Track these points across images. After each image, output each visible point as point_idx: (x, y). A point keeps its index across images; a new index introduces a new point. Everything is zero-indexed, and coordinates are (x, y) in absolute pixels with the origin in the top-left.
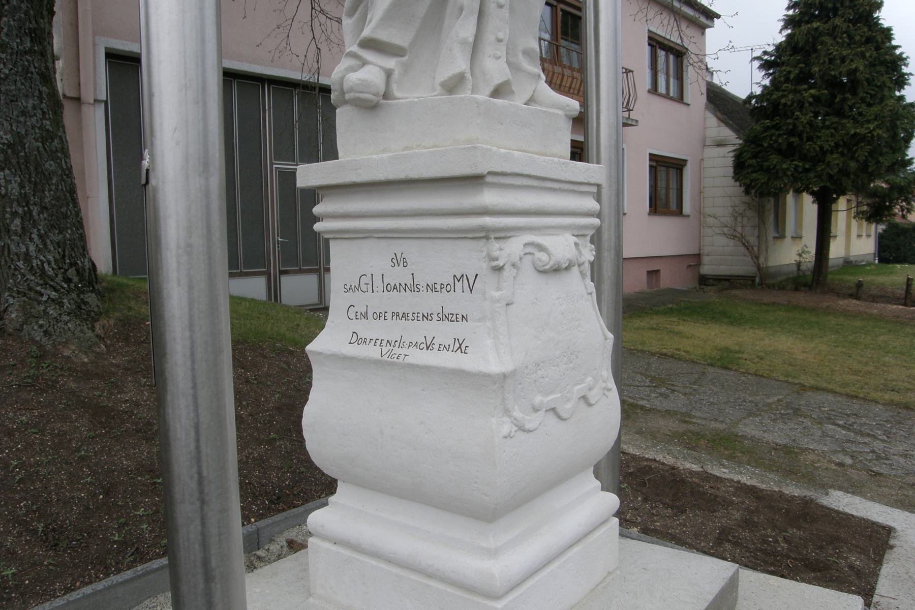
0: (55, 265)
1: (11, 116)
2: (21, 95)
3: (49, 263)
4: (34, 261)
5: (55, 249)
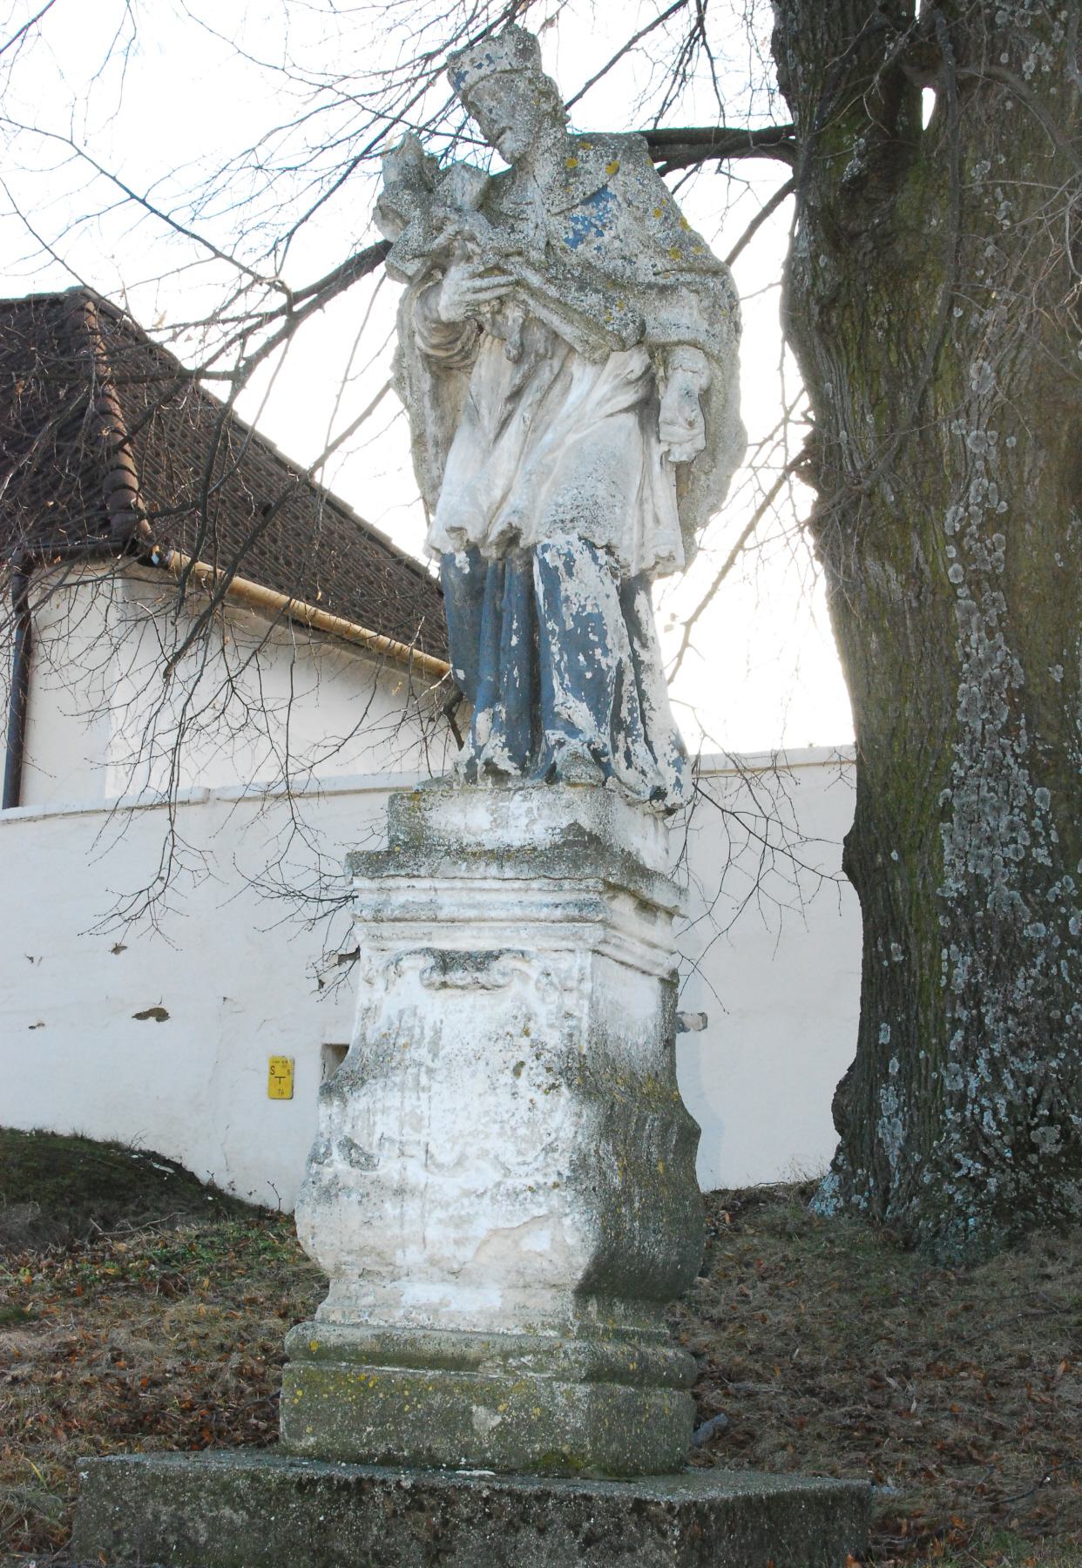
0: (1007, 1116)
2: (987, 809)
3: (995, 1113)
4: (969, 1106)
5: (1017, 1087)
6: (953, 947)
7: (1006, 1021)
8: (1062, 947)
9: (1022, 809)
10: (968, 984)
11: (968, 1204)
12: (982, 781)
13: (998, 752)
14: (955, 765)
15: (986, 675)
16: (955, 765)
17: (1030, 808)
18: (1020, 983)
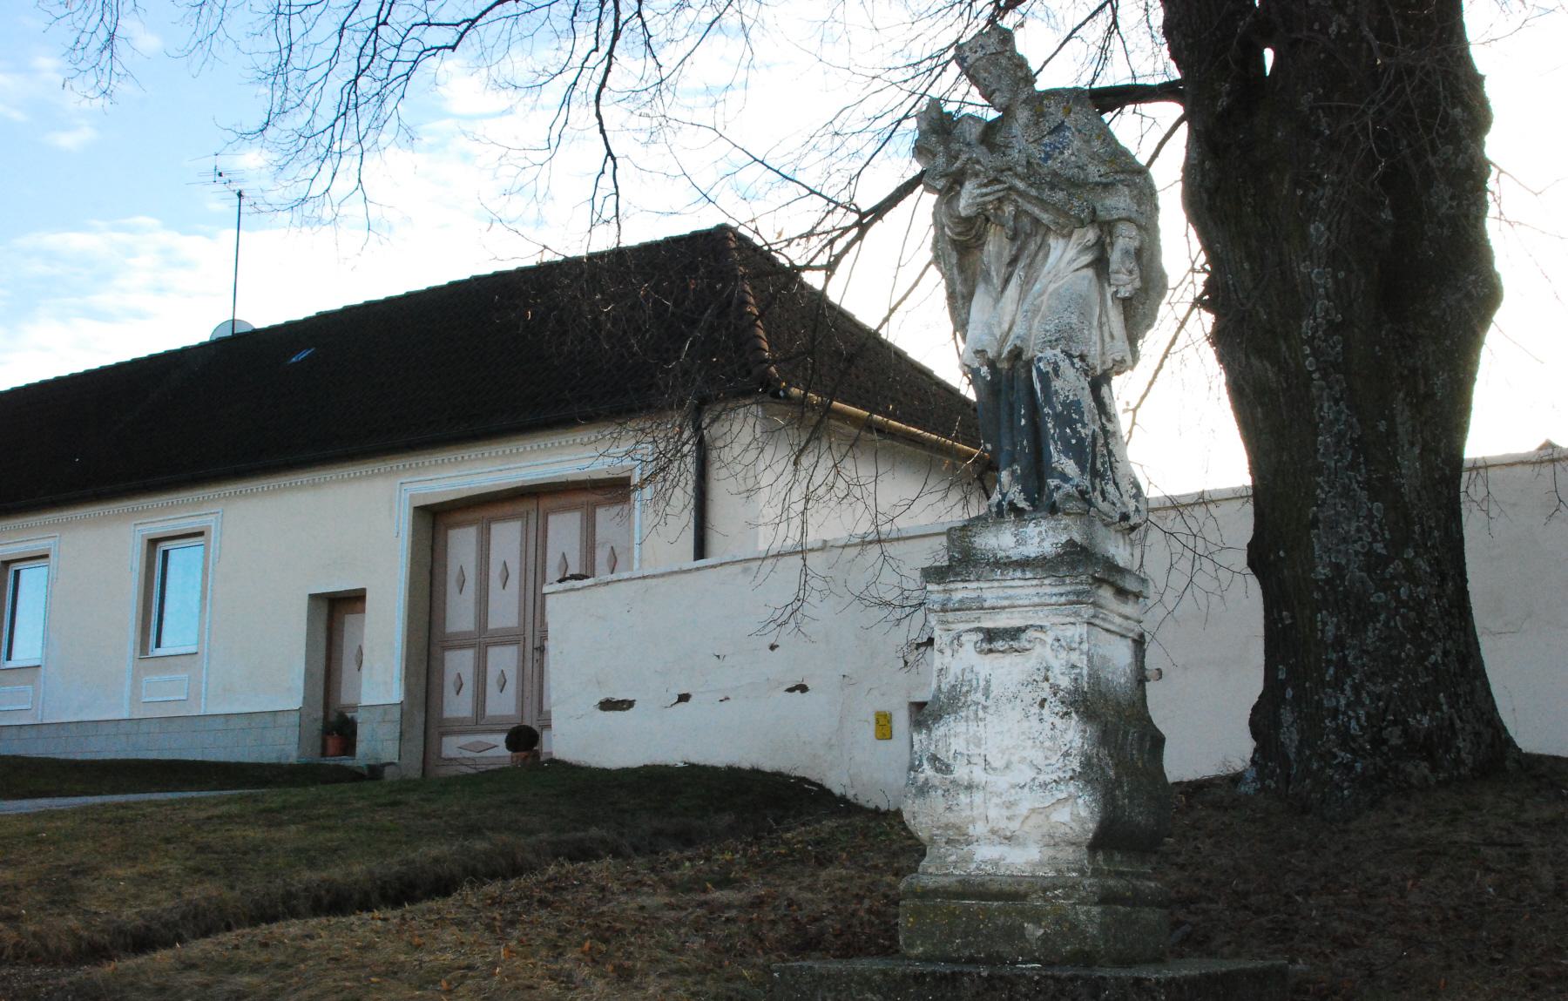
1: (1330, 546)
2: (1341, 519)
4: (1341, 717)
6: (1324, 612)
7: (1362, 659)
8: (1396, 608)
9: (1365, 518)
10: (1336, 636)
11: (1344, 781)
12: (1337, 500)
13: (1347, 481)
14: (1319, 491)
15: (1335, 430)
16: (1319, 491)
17: (1370, 516)
18: (1370, 634)
